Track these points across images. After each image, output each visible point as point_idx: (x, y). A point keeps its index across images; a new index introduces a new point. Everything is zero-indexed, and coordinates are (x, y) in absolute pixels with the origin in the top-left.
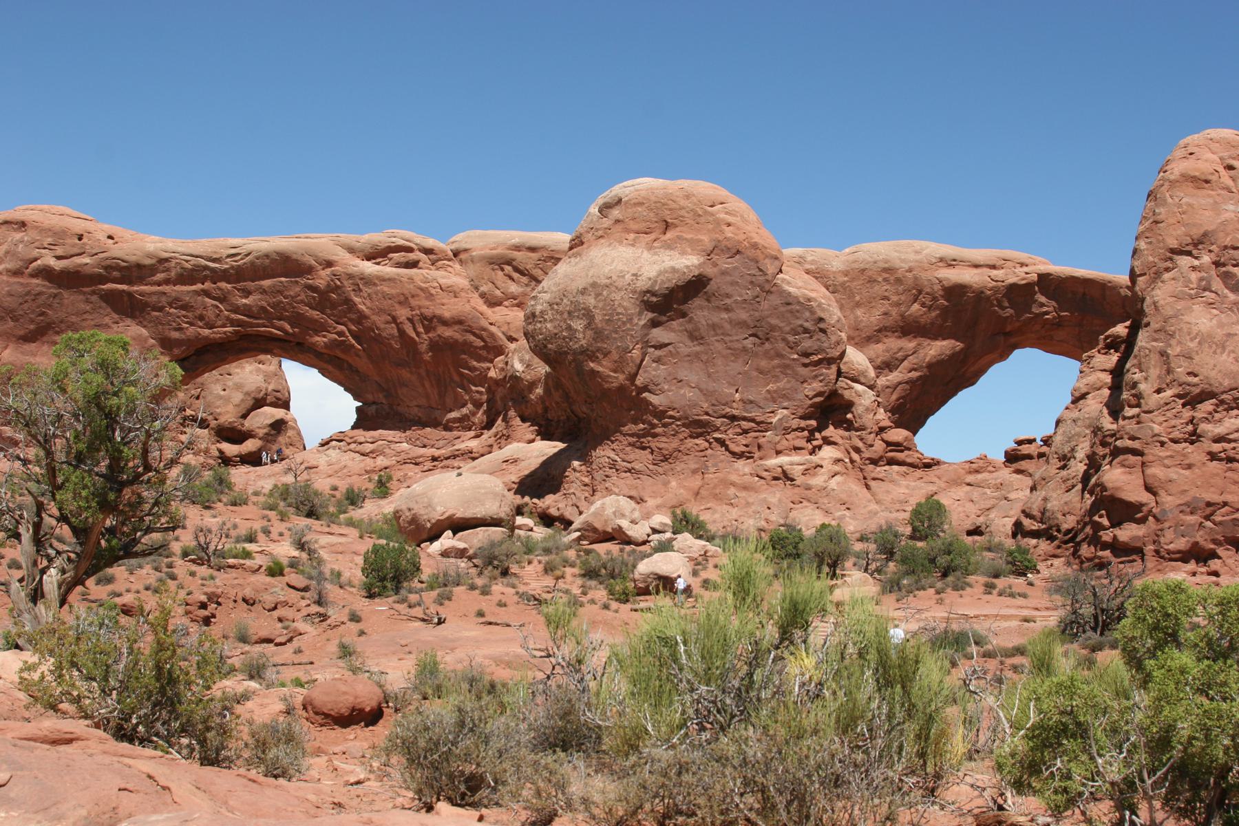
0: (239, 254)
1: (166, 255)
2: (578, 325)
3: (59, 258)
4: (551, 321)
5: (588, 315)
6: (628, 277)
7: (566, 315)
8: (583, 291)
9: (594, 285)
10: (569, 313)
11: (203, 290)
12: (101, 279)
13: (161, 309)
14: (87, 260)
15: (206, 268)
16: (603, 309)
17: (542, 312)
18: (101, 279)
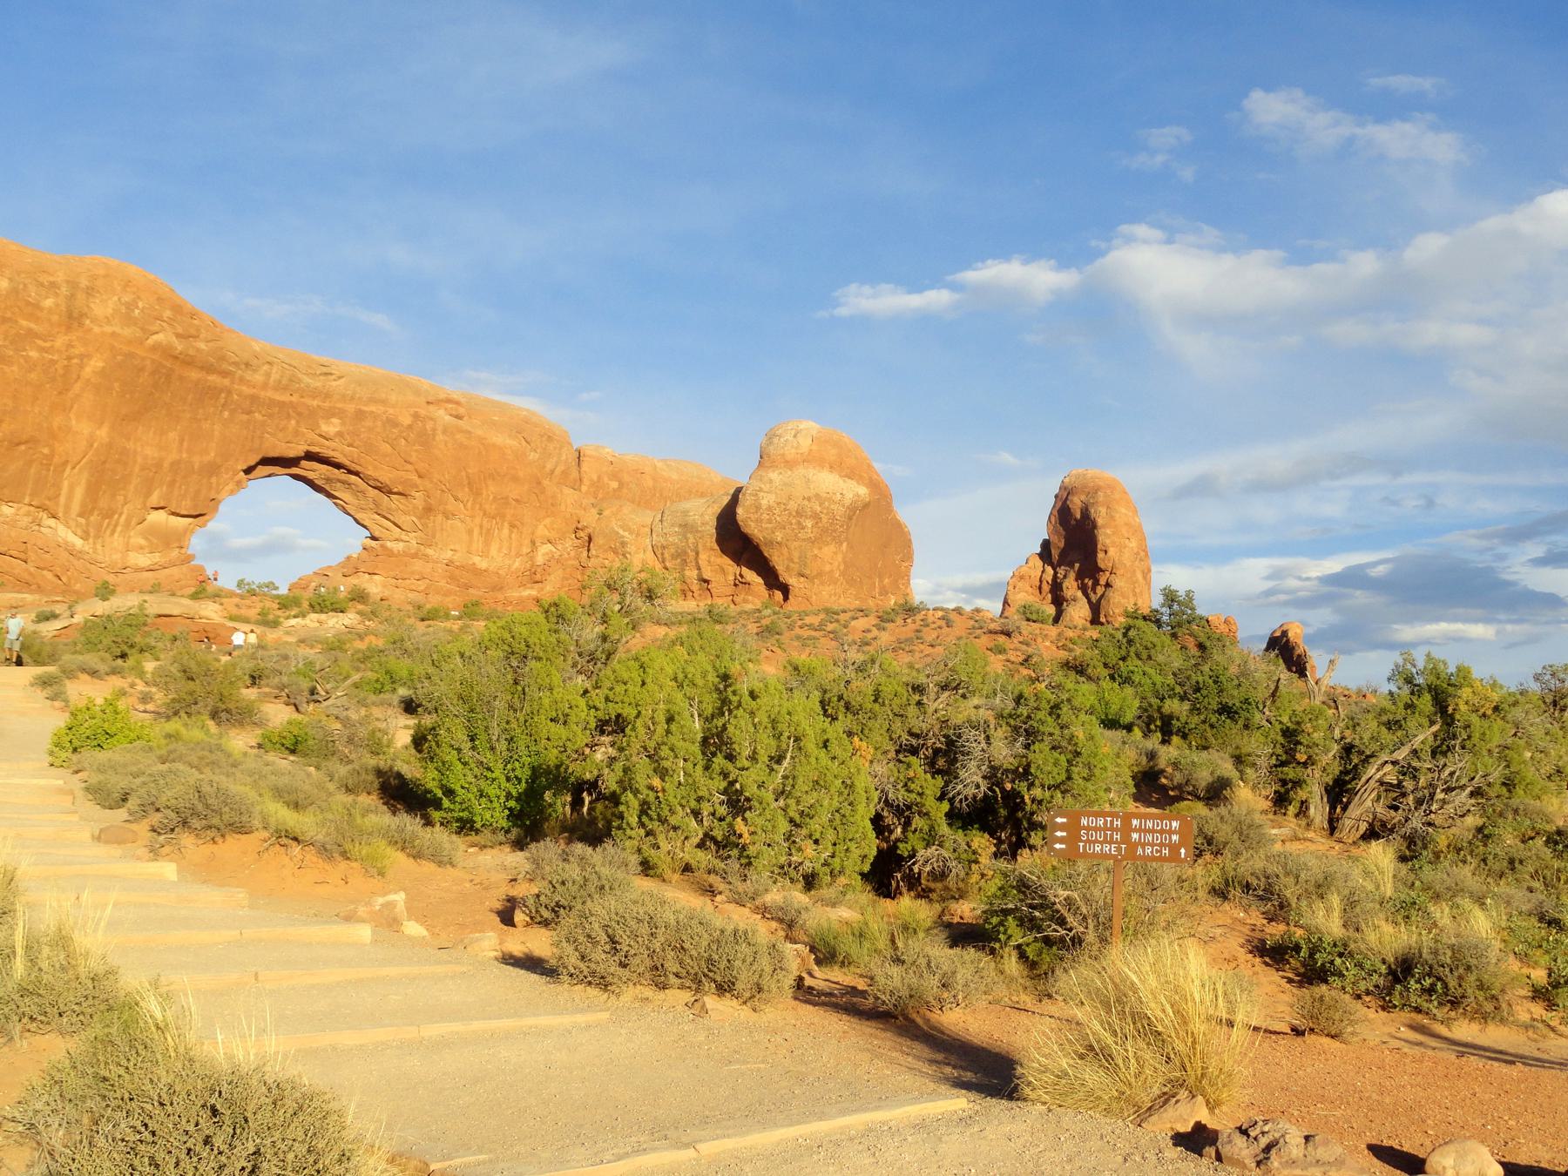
0: (331, 374)
1: (269, 359)
2: (809, 523)
3: (178, 336)
4: (779, 516)
5: (816, 517)
6: (839, 496)
7: (794, 514)
8: (809, 499)
9: (817, 496)
10: (797, 512)
11: (291, 402)
12: (209, 369)
13: (249, 413)
14: (202, 346)
15: (300, 381)
16: (827, 514)
17: (770, 508)
18: (209, 369)
